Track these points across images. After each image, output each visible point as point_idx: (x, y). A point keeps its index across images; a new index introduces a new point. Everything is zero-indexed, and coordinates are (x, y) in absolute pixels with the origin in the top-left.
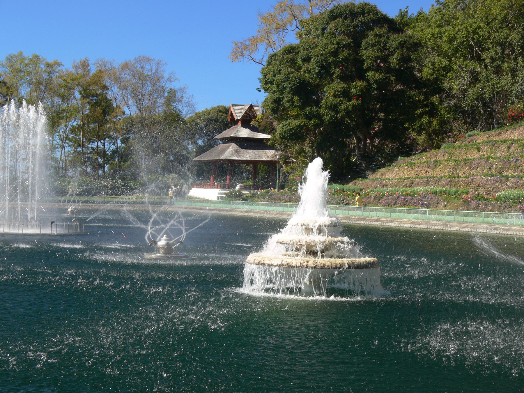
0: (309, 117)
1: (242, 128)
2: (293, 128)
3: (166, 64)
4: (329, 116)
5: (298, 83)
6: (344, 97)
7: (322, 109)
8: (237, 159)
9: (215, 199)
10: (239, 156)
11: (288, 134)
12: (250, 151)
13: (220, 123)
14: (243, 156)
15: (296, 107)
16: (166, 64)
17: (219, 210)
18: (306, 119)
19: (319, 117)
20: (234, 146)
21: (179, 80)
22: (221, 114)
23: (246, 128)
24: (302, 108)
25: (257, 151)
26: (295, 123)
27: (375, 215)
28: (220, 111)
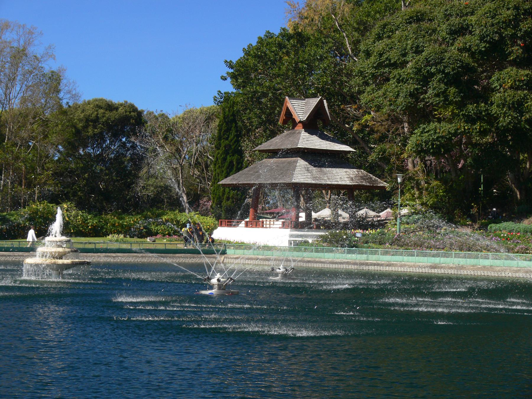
0: (470, 120)
1: (307, 134)
2: (442, 137)
3: (41, 34)
4: (508, 120)
5: (459, 67)
6: (529, 90)
7: (494, 107)
8: (313, 182)
9: (285, 244)
10: (315, 178)
11: (433, 145)
12: (324, 169)
13: (103, 125)
14: (320, 178)
15: (451, 103)
16: (41, 34)
17: (362, 264)
18: (466, 122)
19: (492, 119)
20: (301, 163)
21: (54, 59)
22: (102, 111)
23: (312, 134)
24: (461, 105)
25: (335, 171)
26: (445, 128)
27: (373, 259)
28: (100, 107)
